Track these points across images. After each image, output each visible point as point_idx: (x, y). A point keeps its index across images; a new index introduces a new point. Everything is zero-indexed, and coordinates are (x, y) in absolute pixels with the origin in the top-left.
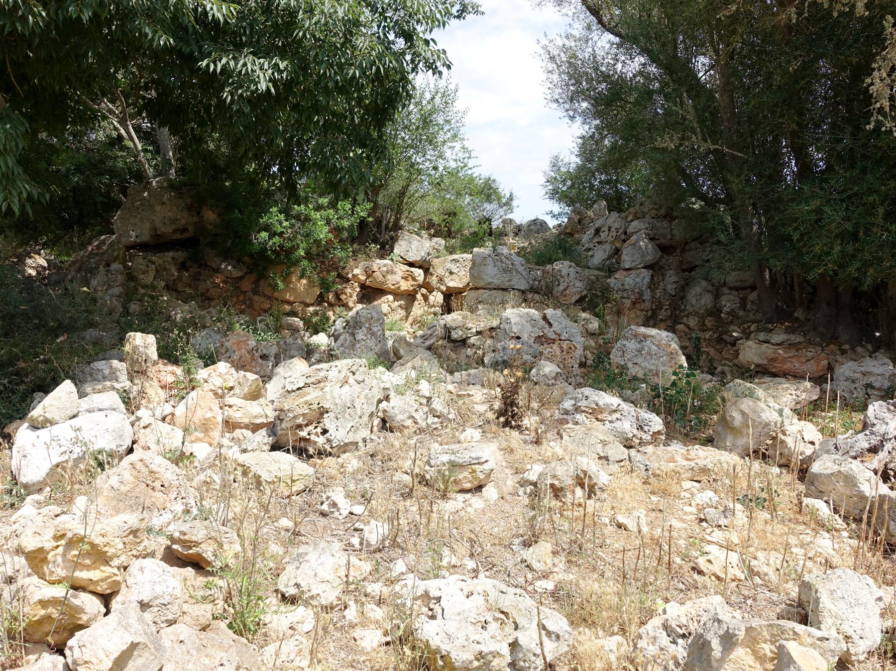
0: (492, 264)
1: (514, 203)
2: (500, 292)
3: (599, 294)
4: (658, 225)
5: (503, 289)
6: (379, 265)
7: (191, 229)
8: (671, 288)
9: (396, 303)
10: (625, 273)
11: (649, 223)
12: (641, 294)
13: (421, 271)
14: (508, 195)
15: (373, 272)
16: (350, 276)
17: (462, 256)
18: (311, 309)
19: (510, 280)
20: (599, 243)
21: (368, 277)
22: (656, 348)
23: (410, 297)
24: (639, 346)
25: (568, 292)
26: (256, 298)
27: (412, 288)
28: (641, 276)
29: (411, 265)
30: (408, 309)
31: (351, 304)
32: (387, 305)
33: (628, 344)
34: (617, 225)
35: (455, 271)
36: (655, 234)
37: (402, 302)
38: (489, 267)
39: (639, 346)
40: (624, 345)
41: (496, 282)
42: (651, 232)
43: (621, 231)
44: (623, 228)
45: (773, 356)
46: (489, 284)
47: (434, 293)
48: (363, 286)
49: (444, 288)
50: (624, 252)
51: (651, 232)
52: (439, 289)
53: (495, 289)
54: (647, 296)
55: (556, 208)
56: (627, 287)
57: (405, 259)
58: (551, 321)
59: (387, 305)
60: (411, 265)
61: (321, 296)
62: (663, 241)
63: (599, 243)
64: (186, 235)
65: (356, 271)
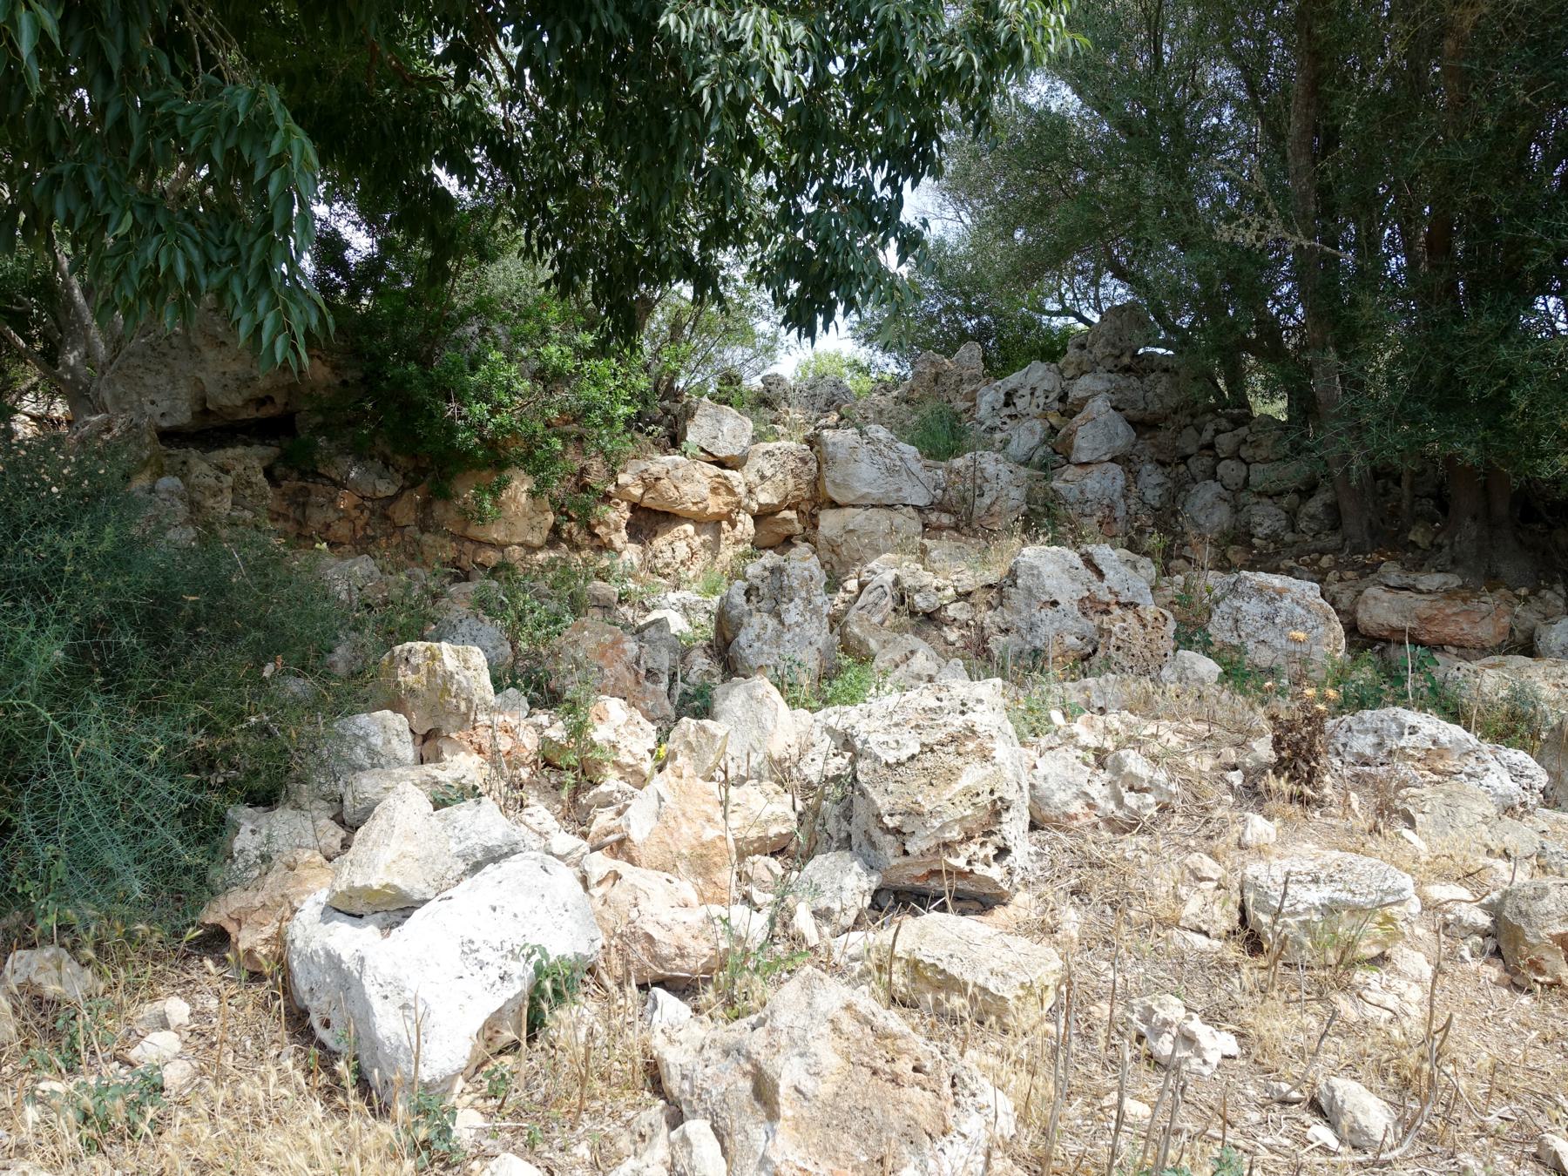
0: (867, 461)
3: (1041, 509)
4: (1123, 384)
5: (890, 507)
6: (661, 463)
7: (280, 400)
8: (1153, 496)
10: (1079, 471)
11: (1110, 381)
12: (1111, 507)
15: (658, 479)
17: (778, 444)
18: (540, 556)
19: (900, 489)
20: (1010, 416)
22: (1303, 612)
24: (1268, 609)
25: (996, 508)
26: (428, 539)
28: (1110, 474)
33: (1245, 607)
34: (1046, 385)
35: (768, 473)
36: (1119, 401)
39: (1268, 609)
40: (1239, 609)
41: (876, 493)
42: (1113, 397)
43: (1053, 396)
44: (1058, 390)
45: (1429, 612)
46: (863, 497)
48: (635, 507)
51: (1113, 397)
54: (1120, 513)
56: (1091, 497)
57: (711, 454)
58: (1102, 567)
61: (555, 529)
62: (1130, 412)
63: (1010, 416)
64: (268, 411)
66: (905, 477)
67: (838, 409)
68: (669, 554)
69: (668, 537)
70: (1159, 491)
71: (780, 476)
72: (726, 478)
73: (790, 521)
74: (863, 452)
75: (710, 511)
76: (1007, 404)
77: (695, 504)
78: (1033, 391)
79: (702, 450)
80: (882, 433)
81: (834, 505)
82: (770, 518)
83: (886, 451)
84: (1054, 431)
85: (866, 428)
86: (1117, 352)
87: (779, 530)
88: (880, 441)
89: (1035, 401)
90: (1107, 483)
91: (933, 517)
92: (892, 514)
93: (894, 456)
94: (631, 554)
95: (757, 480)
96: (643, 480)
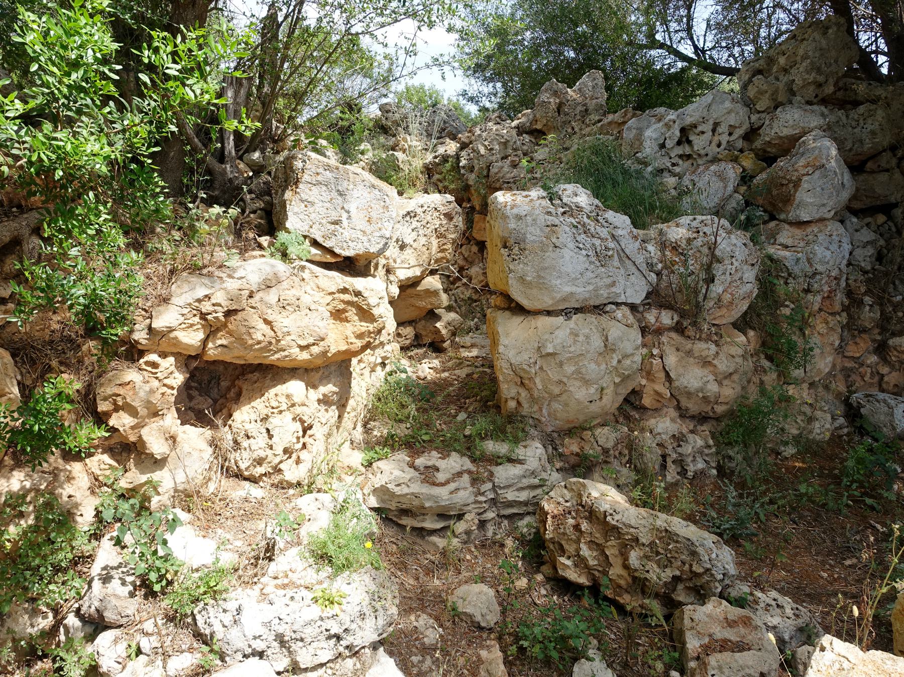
0: (571, 245)
2: (592, 318)
5: (598, 309)
10: (798, 232)
11: (823, 115)
16: (140, 336)
19: (613, 284)
20: (681, 156)
21: (212, 330)
31: (156, 446)
32: (288, 416)
34: (732, 120)
35: (408, 240)
41: (581, 292)
43: (739, 132)
44: (746, 126)
46: (564, 300)
50: (805, 185)
53: (577, 310)
55: (476, 86)
56: (820, 268)
57: (330, 251)
59: (288, 416)
63: (681, 156)
65: (165, 319)
66: (616, 263)
67: (454, 138)
68: (259, 443)
69: (259, 404)
70: (870, 251)
71: (423, 240)
72: (358, 294)
73: (435, 293)
74: (565, 235)
75: (333, 350)
76: (679, 143)
77: (302, 348)
78: (716, 125)
79: (315, 243)
80: (583, 198)
81: (518, 309)
83: (592, 225)
84: (745, 178)
86: (821, 79)
87: (422, 304)
88: (580, 209)
89: (716, 138)
90: (834, 247)
91: (651, 317)
92: (604, 319)
93: (604, 232)
94: (186, 451)
96: (203, 316)
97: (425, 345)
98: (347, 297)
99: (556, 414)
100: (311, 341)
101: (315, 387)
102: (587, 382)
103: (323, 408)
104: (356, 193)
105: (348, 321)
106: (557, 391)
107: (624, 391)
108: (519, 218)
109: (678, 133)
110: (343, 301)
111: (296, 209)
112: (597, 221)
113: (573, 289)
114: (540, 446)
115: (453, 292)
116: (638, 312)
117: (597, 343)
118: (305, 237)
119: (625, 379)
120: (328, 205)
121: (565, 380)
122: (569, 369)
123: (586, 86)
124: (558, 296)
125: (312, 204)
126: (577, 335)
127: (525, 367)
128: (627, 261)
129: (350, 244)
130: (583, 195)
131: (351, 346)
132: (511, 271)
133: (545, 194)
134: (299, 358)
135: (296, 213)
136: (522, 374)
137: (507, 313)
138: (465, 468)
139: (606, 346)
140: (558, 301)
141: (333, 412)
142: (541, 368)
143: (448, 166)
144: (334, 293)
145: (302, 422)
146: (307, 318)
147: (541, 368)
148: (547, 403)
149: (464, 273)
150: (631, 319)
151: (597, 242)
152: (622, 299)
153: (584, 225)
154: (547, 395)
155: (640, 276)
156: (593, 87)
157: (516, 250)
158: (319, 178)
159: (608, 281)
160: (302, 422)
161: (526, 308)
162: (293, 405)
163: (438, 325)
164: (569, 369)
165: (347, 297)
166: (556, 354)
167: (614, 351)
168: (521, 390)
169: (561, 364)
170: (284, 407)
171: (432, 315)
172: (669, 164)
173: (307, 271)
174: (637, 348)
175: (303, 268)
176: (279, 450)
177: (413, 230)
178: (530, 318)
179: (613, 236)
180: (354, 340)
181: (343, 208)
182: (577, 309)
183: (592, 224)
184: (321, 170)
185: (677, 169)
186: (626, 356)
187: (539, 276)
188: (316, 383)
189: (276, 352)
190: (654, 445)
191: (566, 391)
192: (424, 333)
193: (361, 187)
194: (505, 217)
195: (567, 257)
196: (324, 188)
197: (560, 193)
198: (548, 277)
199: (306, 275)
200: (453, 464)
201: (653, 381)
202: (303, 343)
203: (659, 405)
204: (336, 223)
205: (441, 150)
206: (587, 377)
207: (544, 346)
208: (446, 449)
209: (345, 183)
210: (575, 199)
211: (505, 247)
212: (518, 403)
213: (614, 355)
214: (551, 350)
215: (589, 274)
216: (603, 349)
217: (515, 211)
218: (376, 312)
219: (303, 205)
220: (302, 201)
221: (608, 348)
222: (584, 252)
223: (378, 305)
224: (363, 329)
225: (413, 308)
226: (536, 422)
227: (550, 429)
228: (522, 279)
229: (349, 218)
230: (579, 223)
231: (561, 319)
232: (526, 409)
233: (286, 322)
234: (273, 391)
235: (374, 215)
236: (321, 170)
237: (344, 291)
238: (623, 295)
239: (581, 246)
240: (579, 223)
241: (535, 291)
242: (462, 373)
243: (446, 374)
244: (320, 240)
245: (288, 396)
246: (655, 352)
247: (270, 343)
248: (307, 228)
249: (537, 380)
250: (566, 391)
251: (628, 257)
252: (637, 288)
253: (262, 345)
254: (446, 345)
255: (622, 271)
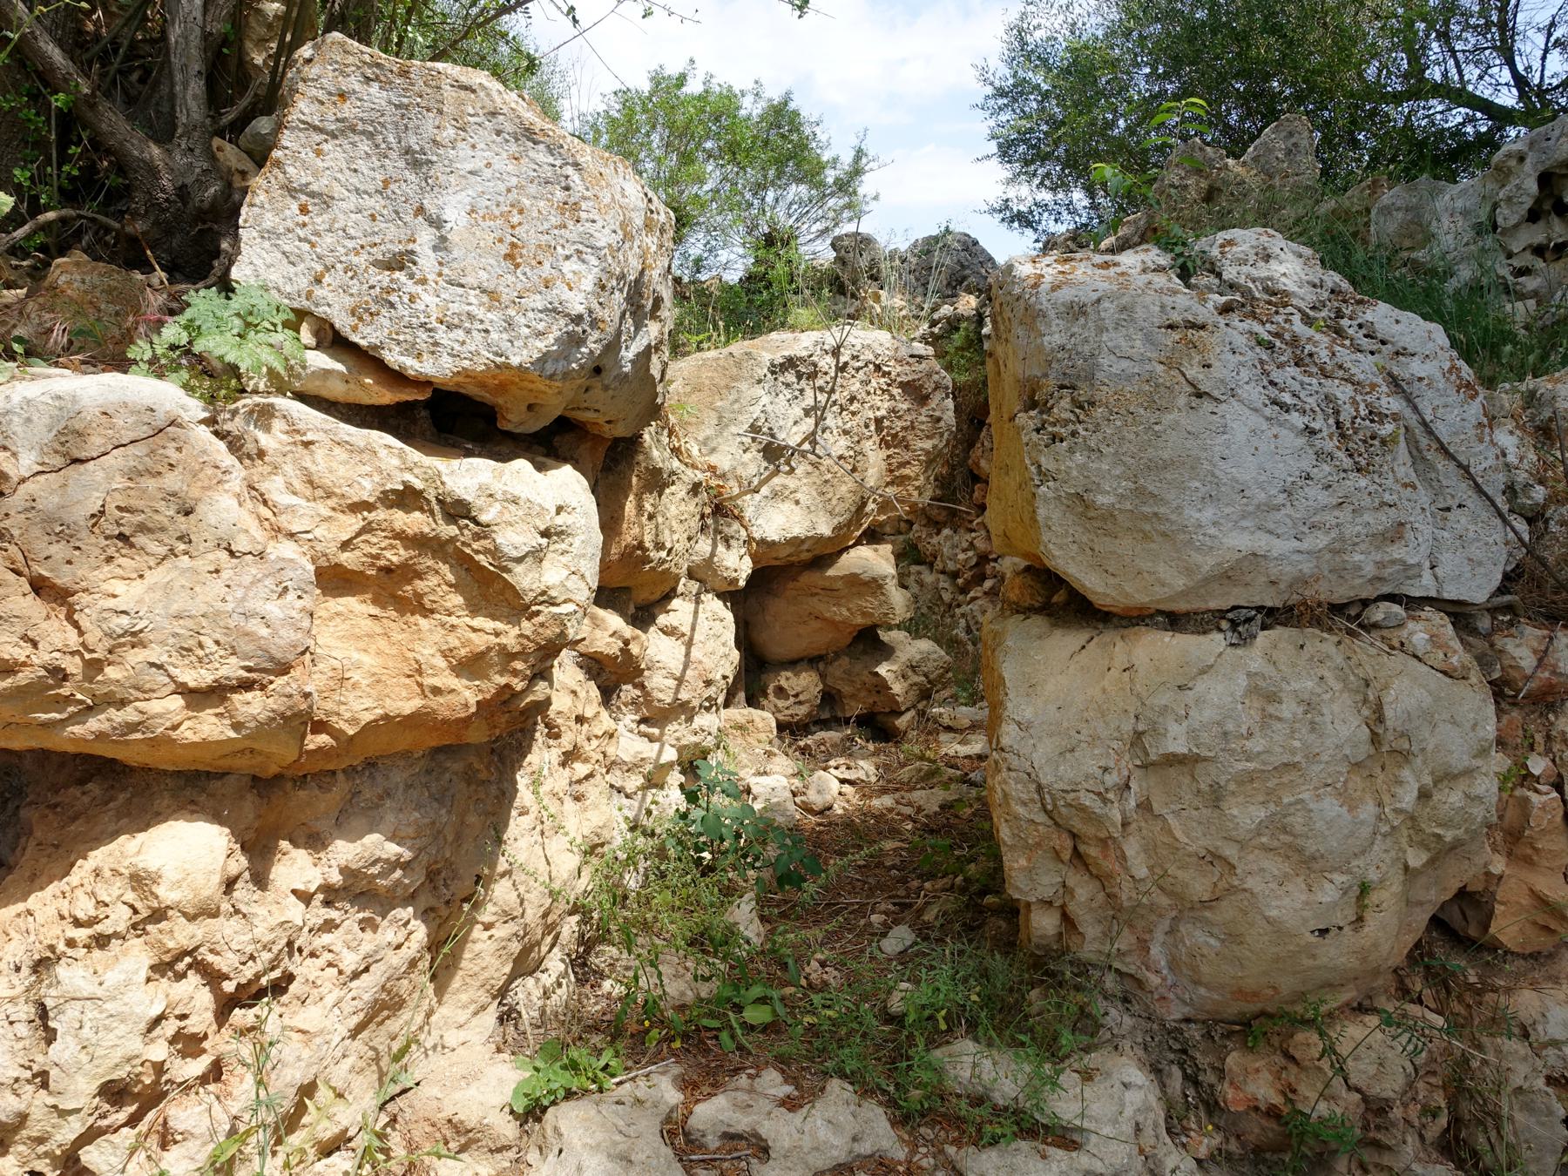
0: (1254, 393)
1: (866, 186)
2: (1323, 644)
9: (296, 868)
13: (565, 488)
14: (847, 159)
19: (1397, 532)
20: (1539, 251)
23: (460, 770)
27: (466, 694)
29: (453, 417)
30: (445, 889)
32: (136, 957)
35: (792, 436)
37: (368, 848)
38: (1241, 421)
41: (1289, 554)
46: (1227, 576)
47: (679, 612)
49: (737, 564)
52: (704, 575)
53: (1273, 616)
57: (367, 359)
59: (136, 957)
60: (453, 417)
63: (1539, 251)
72: (457, 510)
73: (874, 585)
76: (1534, 216)
77: (197, 698)
79: (332, 340)
80: (1291, 268)
82: (807, 578)
83: (1321, 344)
85: (1210, 244)
87: (840, 612)
88: (1278, 297)
92: (1366, 649)
93: (1364, 367)
95: (752, 464)
97: (847, 721)
98: (414, 522)
99: (1195, 965)
100: (232, 669)
101: (315, 842)
102: (1308, 864)
103: (350, 917)
104: (465, 158)
105: (427, 612)
106: (1199, 886)
107: (1434, 895)
108: (1076, 311)
109: (1532, 186)
110: (400, 536)
111: (269, 221)
112: (1339, 332)
113: (1261, 542)
114: (1137, 1076)
115: (965, 609)
116: (1474, 632)
117: (1344, 726)
118: (301, 314)
119: (1442, 852)
120: (375, 203)
121: (1230, 851)
122: (1246, 814)
123: (1270, 151)
124: (1207, 563)
125: (326, 200)
126: (1273, 698)
127: (1088, 800)
128: (1441, 464)
129: (442, 335)
130: (1290, 256)
131: (436, 702)
132: (1045, 476)
133: (1164, 260)
134: (187, 734)
135: (268, 234)
136: (1077, 824)
137: (1038, 623)
138: (865, 1148)
139: (1375, 739)
140: (1207, 581)
141: (405, 932)
142: (1145, 806)
143: (958, 338)
144: (369, 507)
145: (213, 977)
146: (216, 587)
147: (1145, 806)
148: (1165, 925)
149: (988, 568)
150: (1459, 657)
151: (1343, 393)
152: (1424, 585)
153: (1295, 341)
154: (1164, 901)
155: (1486, 514)
156: (1289, 152)
157: (1062, 409)
158: (348, 110)
159: (1384, 520)
160: (213, 977)
161: (1098, 601)
162: (158, 915)
163: (883, 670)
164: (1246, 814)
165: (414, 522)
166: (1197, 759)
167: (1405, 756)
168: (1075, 879)
169: (1216, 797)
170: (119, 919)
171: (869, 642)
172: (1505, 272)
173: (278, 425)
174: (1483, 752)
175: (264, 416)
176: (81, 1091)
177: (807, 413)
178: (1109, 635)
179: (1395, 382)
180: (448, 680)
181: (420, 210)
182: (1271, 611)
183: (1323, 340)
184: (353, 83)
185: (1530, 283)
186: (1447, 777)
187: (1140, 493)
188: (322, 826)
189: (90, 710)
190: (1540, 1083)
191: (1231, 890)
192: (846, 689)
193: (483, 136)
194: (1033, 316)
195: (1240, 431)
196: (365, 146)
197: (1215, 252)
198: (1170, 496)
199: (271, 440)
200: (824, 1133)
201: (1528, 862)
202: (194, 677)
203: (1543, 942)
204: (399, 262)
205: (946, 310)
206: (1311, 847)
207: (1156, 731)
208: (809, 1065)
209: (431, 120)
210: (1262, 271)
211: (1032, 404)
212: (1066, 919)
213: (1406, 773)
214: (1179, 747)
215: (1314, 493)
216: (1365, 749)
217: (1066, 294)
218: (524, 579)
219: (295, 207)
220: (291, 191)
221: (1385, 746)
222: (1297, 419)
223: (537, 555)
224: (480, 642)
225: (816, 624)
226: (1129, 985)
227: (1175, 1013)
228: (1081, 503)
229: (441, 244)
230: (1277, 335)
231: (1216, 642)
232: (1091, 943)
233: (128, 594)
234: (99, 857)
235: (529, 235)
236: (353, 83)
237: (407, 498)
238: (1427, 576)
239: (1287, 398)
240: (1277, 335)
241: (1125, 545)
242: (930, 799)
243: (887, 801)
244: (342, 322)
245: (140, 881)
246: (1538, 765)
247: (59, 674)
248: (304, 283)
249: (1132, 848)
250: (1231, 890)
251: (1443, 449)
252: (1475, 551)
253: (23, 678)
254: (902, 722)
255: (1423, 496)
